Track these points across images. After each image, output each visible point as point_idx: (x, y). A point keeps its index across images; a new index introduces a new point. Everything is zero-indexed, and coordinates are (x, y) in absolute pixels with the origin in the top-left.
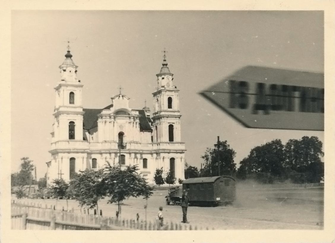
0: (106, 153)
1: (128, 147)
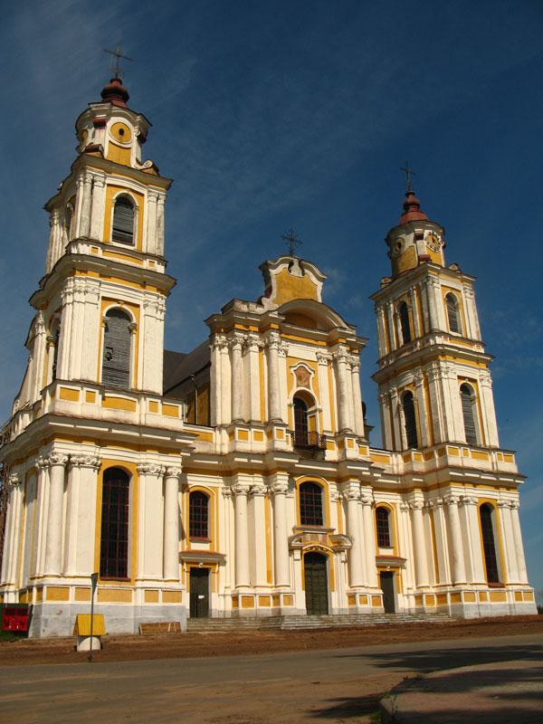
0: (251, 470)
1: (332, 454)
